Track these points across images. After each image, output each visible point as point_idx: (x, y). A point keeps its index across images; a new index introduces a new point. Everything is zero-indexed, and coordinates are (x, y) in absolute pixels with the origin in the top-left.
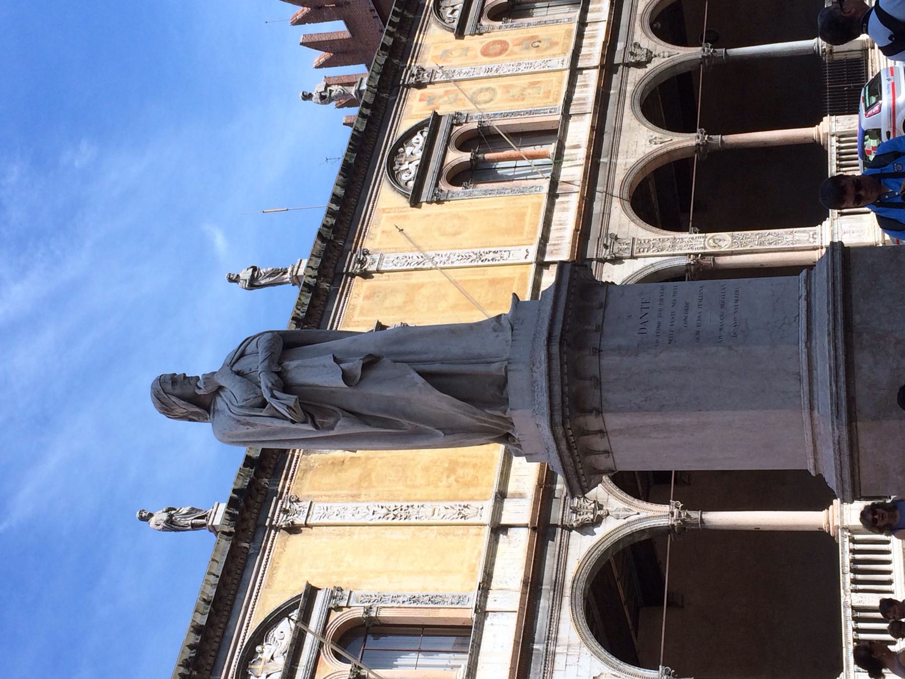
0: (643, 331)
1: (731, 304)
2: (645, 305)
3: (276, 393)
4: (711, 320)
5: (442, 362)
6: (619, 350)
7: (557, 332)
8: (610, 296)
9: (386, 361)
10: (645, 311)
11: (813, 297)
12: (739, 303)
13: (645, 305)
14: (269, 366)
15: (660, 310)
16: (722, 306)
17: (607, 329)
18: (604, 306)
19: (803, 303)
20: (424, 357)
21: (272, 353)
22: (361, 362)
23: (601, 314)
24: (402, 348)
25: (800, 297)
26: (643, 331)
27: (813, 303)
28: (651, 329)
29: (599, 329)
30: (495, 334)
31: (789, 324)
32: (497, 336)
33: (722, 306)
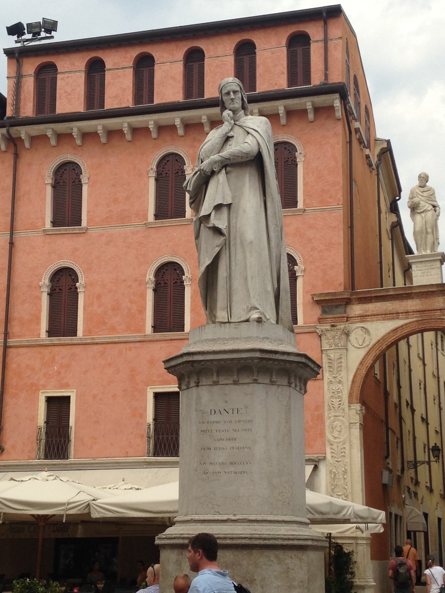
0: (213, 412)
1: (232, 469)
2: (235, 411)
3: (199, 173)
4: (220, 457)
5: (230, 277)
6: (199, 398)
7: (196, 358)
8: (245, 386)
9: (220, 240)
10: (230, 412)
11: (231, 524)
12: (233, 474)
13: (235, 411)
14: (216, 162)
15: (230, 422)
16: (231, 463)
17: (216, 388)
18: (236, 383)
19: (225, 517)
20: (233, 263)
21: (229, 159)
22: (211, 225)
23: (228, 382)
24: (238, 246)
25: (235, 515)
26: (213, 412)
27: (227, 524)
28: (213, 418)
29: (216, 383)
30: (246, 309)
31: (213, 508)
32: (244, 310)
33: (231, 463)
